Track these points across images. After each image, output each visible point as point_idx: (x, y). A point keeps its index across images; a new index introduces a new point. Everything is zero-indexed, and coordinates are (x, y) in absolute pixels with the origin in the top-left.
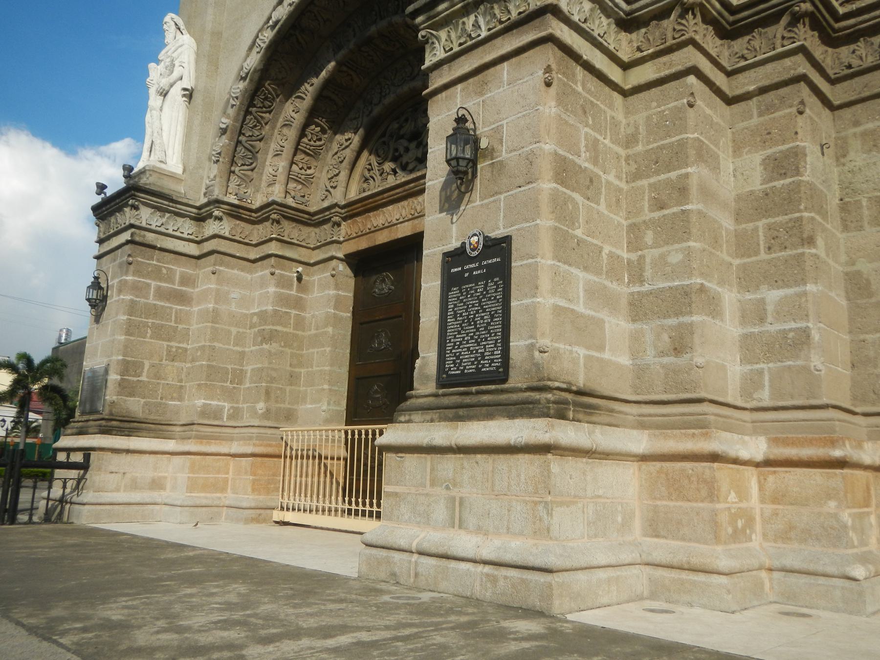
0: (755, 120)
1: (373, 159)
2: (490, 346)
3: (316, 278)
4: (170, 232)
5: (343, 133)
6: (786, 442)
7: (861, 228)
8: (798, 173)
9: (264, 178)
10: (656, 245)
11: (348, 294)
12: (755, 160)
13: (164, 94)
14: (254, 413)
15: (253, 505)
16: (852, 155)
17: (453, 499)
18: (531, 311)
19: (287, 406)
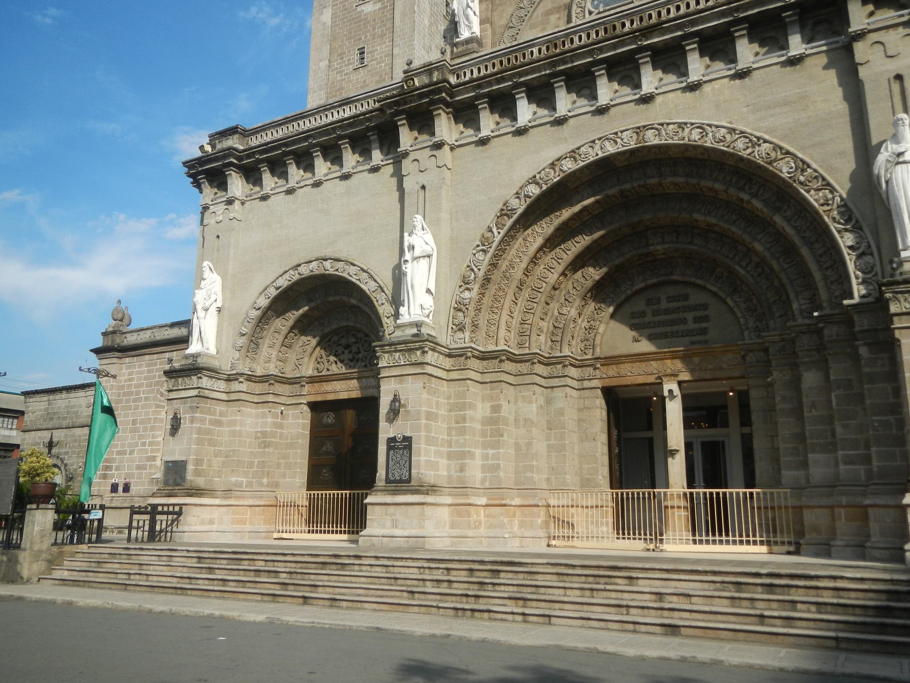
0: (488, 392)
1: (323, 352)
2: (405, 471)
3: (290, 412)
4: (215, 389)
5: (306, 336)
6: (492, 499)
7: (519, 428)
8: (499, 413)
9: (262, 357)
10: (456, 436)
11: (308, 422)
12: (488, 405)
13: (206, 310)
14: (261, 484)
15: (265, 530)
16: (519, 403)
17: (393, 520)
18: (419, 461)
19: (276, 480)
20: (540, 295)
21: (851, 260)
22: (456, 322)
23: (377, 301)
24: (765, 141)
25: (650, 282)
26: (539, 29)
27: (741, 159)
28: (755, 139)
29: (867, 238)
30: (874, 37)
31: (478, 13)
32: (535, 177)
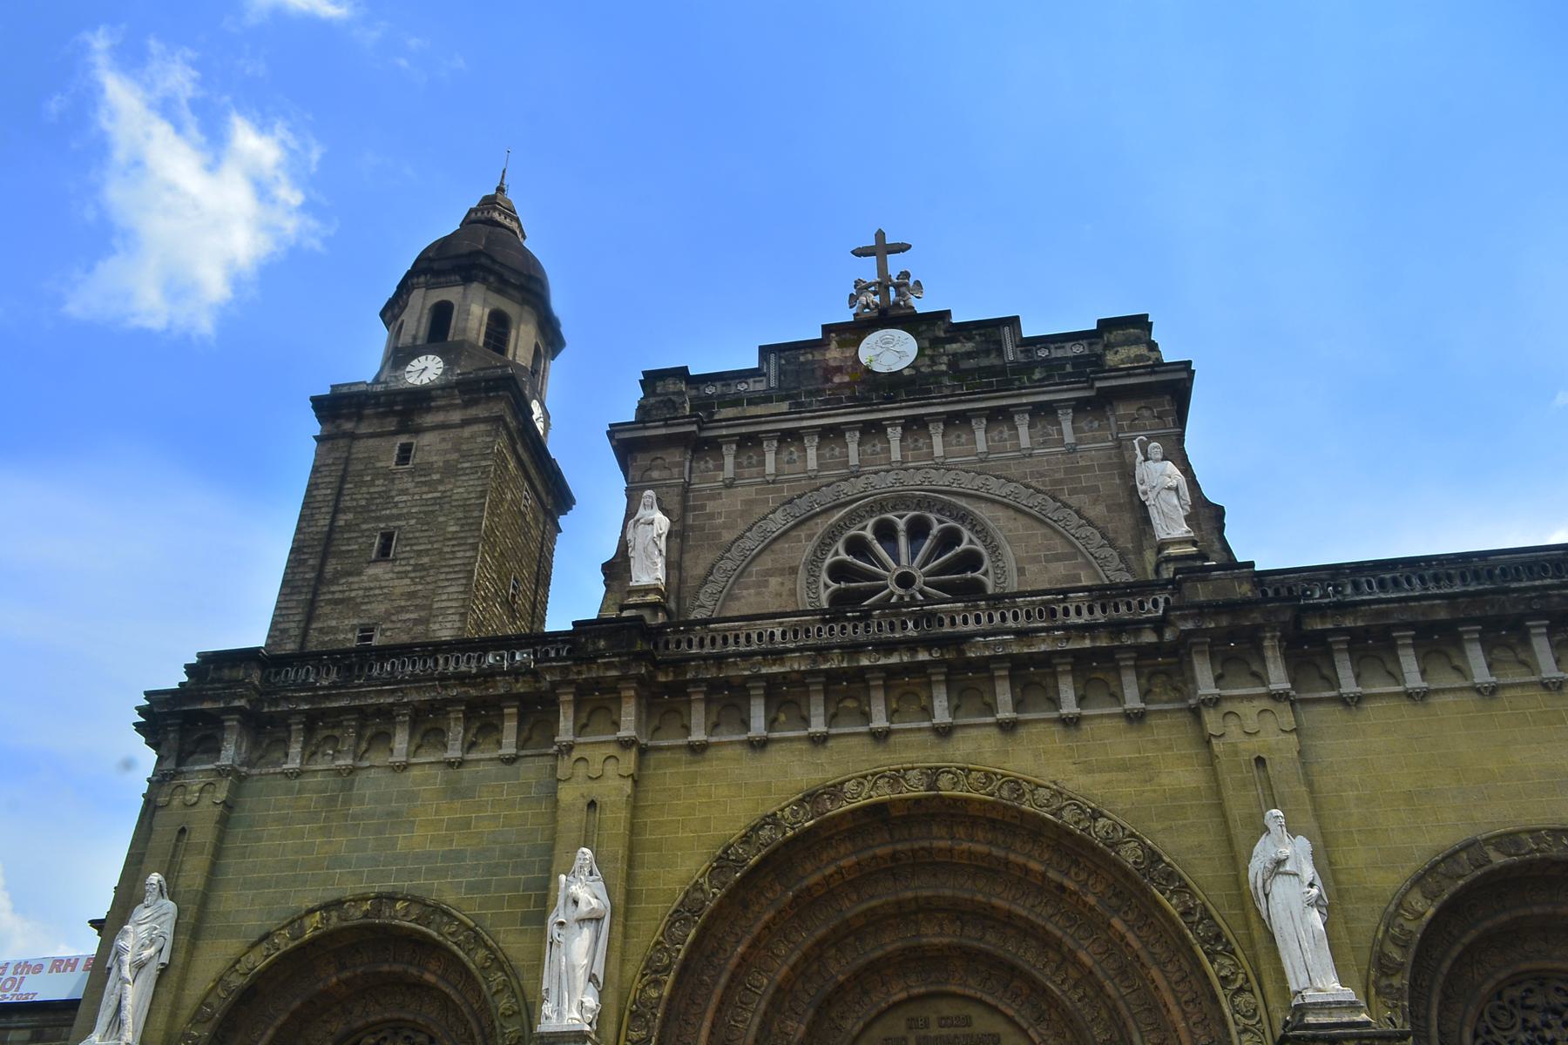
20: (757, 998)
21: (1226, 996)
22: (634, 1035)
23: (489, 988)
24: (1102, 815)
25: (915, 991)
26: (752, 591)
27: (1070, 834)
28: (1089, 810)
29: (1243, 967)
30: (1227, 707)
31: (664, 554)
32: (775, 814)
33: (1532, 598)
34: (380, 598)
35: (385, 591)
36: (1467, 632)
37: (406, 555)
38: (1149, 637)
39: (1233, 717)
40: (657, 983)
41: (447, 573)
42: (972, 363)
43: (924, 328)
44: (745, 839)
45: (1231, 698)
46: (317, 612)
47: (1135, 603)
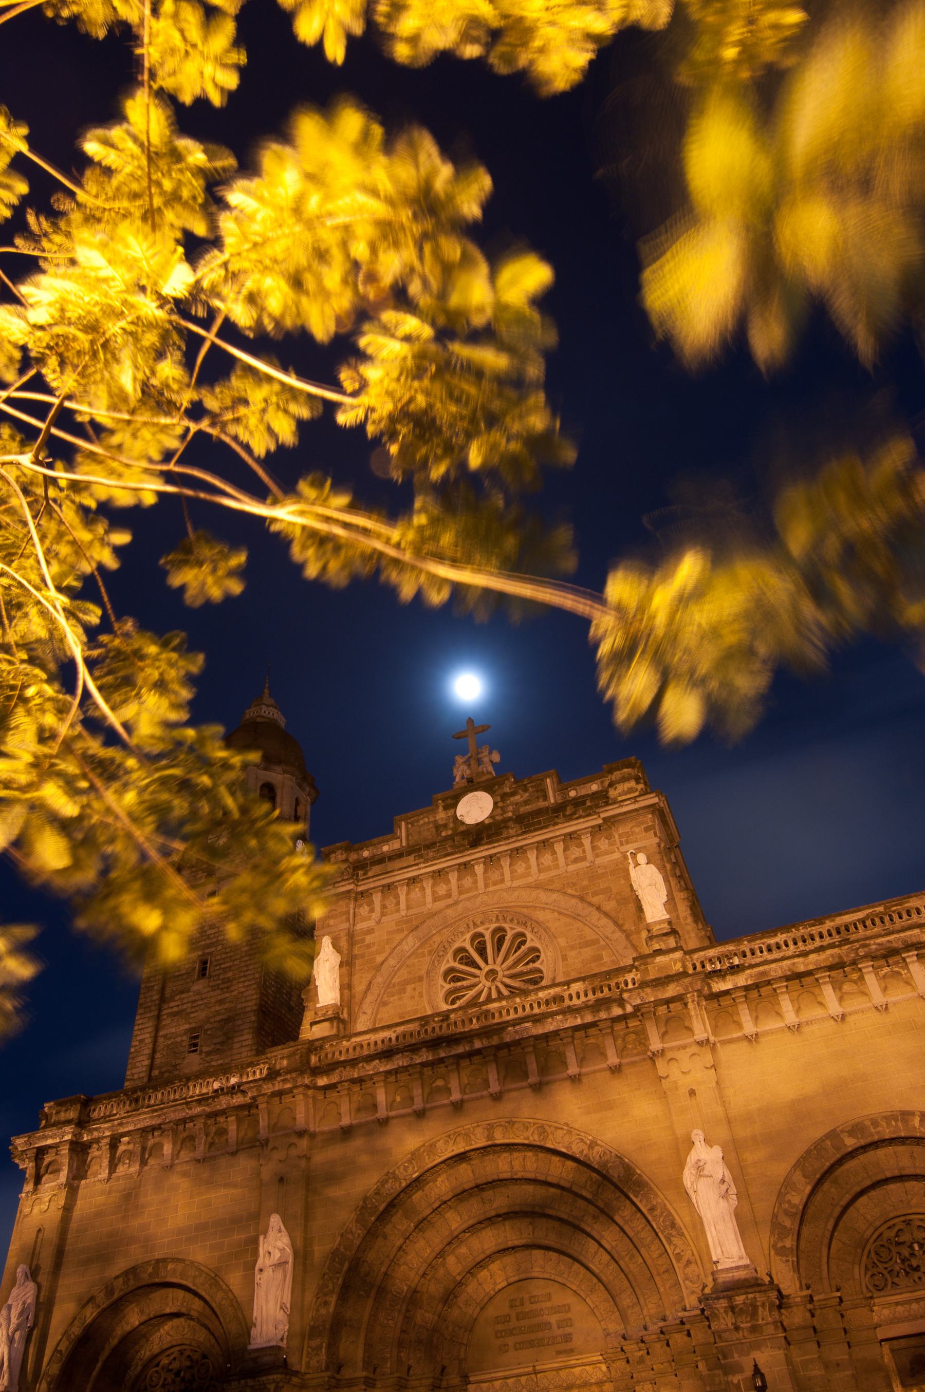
26: (395, 997)
33: (857, 949)
34: (202, 1007)
35: (205, 1001)
36: (821, 978)
37: (217, 972)
38: (617, 1011)
39: (674, 1062)
40: (326, 1303)
41: (243, 982)
42: (529, 808)
43: (497, 787)
44: (377, 1193)
45: (672, 1049)
46: (164, 1023)
47: (613, 984)
